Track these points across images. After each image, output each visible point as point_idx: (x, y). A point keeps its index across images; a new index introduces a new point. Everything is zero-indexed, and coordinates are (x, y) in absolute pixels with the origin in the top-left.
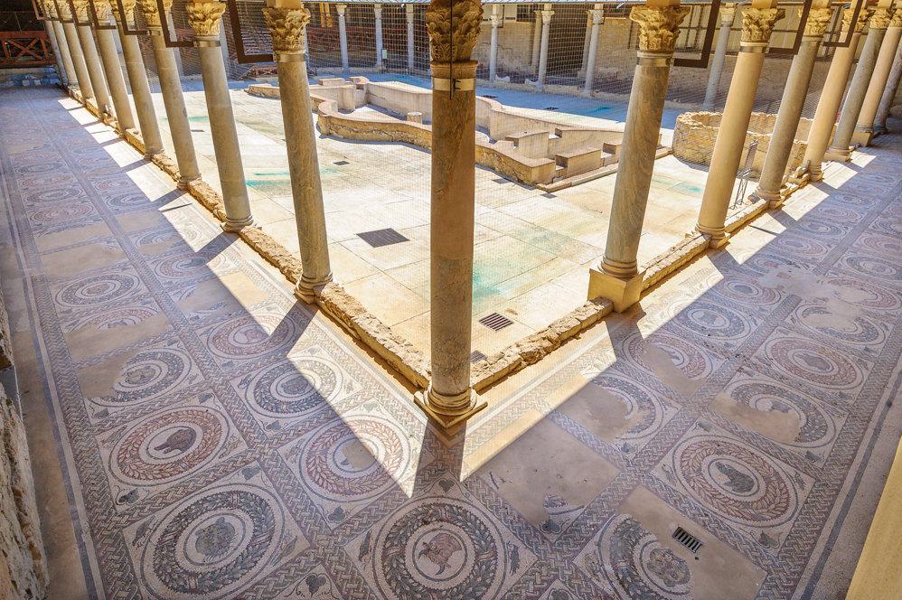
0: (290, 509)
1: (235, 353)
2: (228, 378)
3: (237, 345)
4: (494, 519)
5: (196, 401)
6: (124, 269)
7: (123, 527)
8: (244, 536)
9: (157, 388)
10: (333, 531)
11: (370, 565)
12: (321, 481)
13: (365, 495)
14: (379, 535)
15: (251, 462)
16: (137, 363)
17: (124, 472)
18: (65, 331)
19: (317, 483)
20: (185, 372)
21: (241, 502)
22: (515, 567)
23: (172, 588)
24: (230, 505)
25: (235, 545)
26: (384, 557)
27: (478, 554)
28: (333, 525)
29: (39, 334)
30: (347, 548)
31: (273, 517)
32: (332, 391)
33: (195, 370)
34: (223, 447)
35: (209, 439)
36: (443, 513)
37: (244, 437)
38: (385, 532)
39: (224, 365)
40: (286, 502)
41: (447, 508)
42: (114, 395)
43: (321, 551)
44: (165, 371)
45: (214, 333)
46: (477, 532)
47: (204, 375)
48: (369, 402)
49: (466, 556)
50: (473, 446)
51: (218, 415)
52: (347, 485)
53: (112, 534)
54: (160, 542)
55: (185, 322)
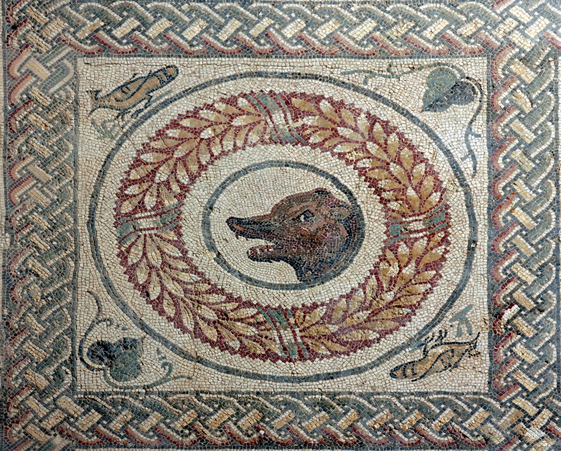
35: (392, 281)
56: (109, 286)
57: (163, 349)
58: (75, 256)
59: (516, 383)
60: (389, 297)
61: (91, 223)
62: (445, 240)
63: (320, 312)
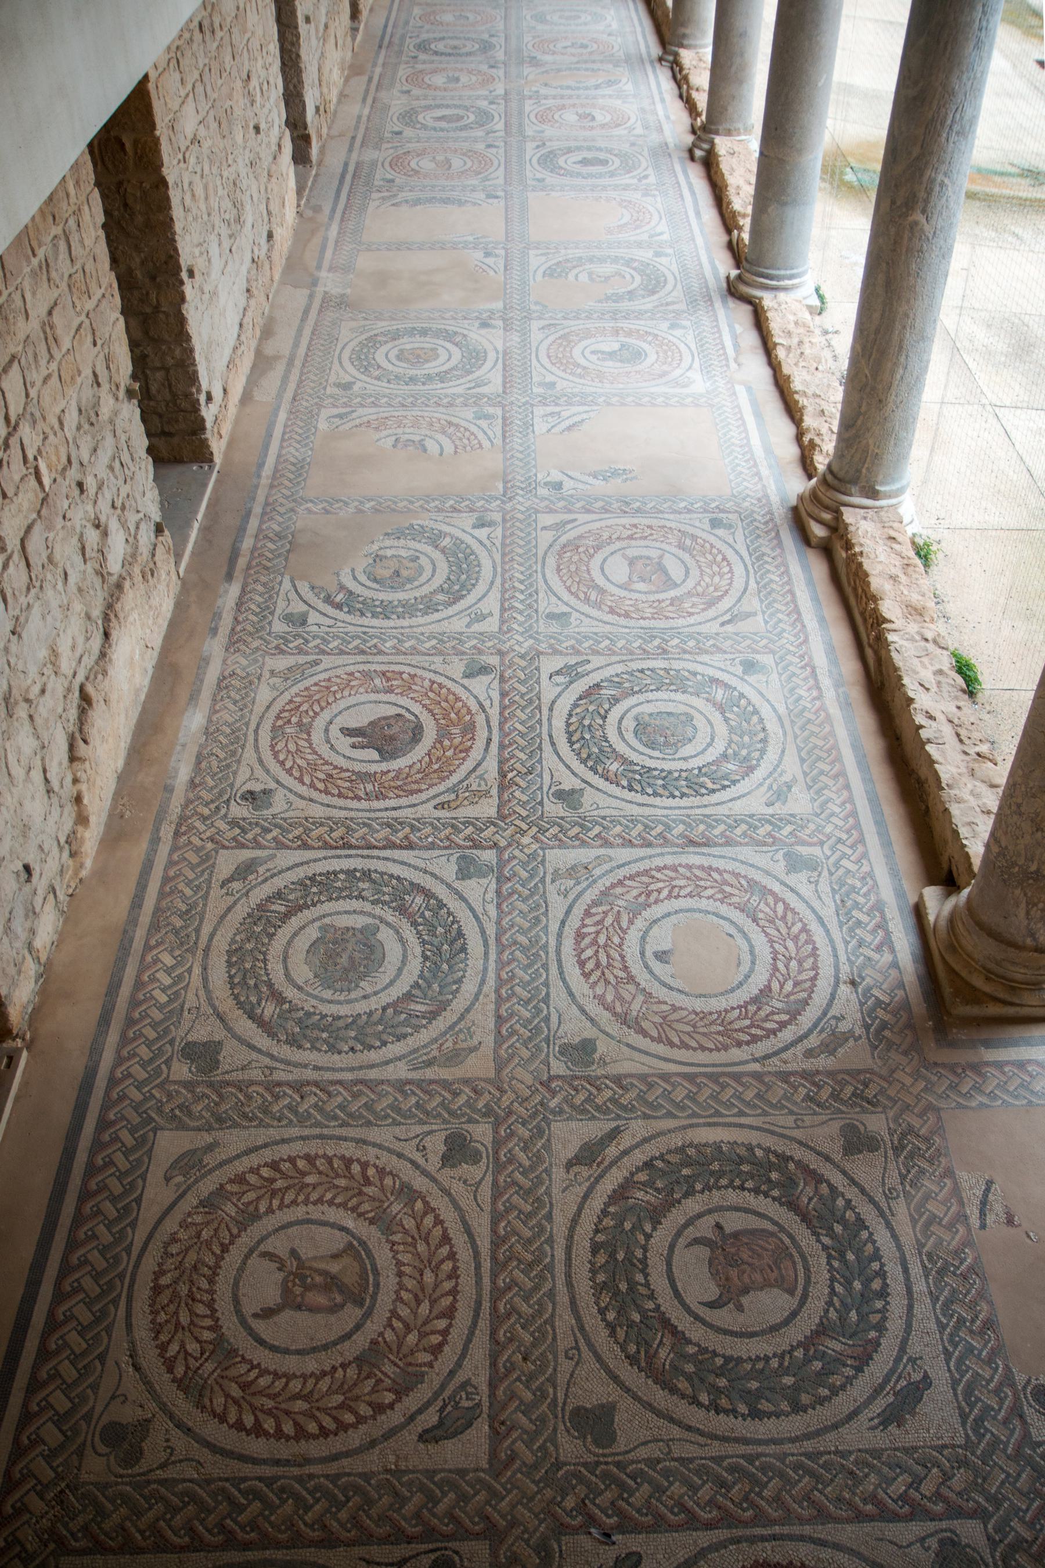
0: (500, 982)
1: (587, 600)
2: (544, 646)
3: (600, 581)
4: (920, 1286)
5: (457, 667)
6: (485, 325)
7: (224, 847)
8: (392, 983)
9: (408, 609)
10: (551, 1079)
11: (580, 1190)
12: (590, 965)
13: (661, 1049)
14: (637, 1146)
15: (484, 848)
16: (402, 542)
17: (272, 747)
18: (323, 425)
19: (582, 964)
20: (470, 599)
21: (422, 916)
22: (892, 1417)
23: (236, 997)
24: (402, 910)
25: (369, 990)
26: (619, 1195)
27: (822, 1330)
28: (558, 1067)
29: (282, 416)
30: (558, 1128)
31: (459, 981)
32: (734, 782)
33: (492, 604)
34: (453, 789)
35: (438, 759)
36: (805, 1192)
37: (502, 788)
38: (652, 1150)
39: (551, 616)
40: (501, 965)
41: (824, 1189)
42: (333, 588)
43: (505, 1102)
44: (438, 580)
45: (572, 535)
46: (857, 1285)
47: (503, 622)
48: (804, 850)
49: (794, 1314)
50: (992, 1096)
51: (480, 719)
52: (636, 1006)
53: (203, 848)
54: (260, 907)
55: (531, 486)
56: (261, 761)
57: (288, 794)
58: (243, 747)
59: (515, 812)
60: (436, 767)
61: (256, 731)
62: (473, 738)
63: (392, 774)
